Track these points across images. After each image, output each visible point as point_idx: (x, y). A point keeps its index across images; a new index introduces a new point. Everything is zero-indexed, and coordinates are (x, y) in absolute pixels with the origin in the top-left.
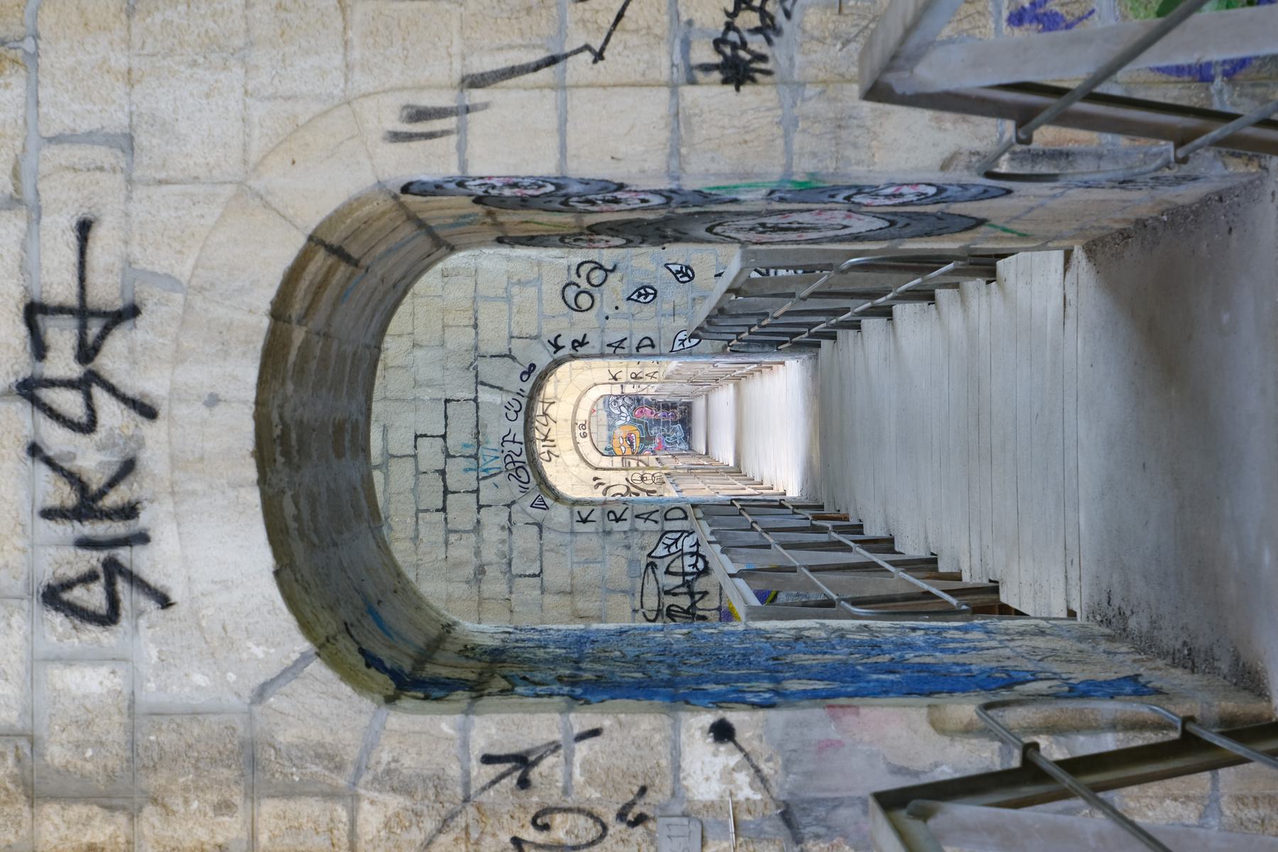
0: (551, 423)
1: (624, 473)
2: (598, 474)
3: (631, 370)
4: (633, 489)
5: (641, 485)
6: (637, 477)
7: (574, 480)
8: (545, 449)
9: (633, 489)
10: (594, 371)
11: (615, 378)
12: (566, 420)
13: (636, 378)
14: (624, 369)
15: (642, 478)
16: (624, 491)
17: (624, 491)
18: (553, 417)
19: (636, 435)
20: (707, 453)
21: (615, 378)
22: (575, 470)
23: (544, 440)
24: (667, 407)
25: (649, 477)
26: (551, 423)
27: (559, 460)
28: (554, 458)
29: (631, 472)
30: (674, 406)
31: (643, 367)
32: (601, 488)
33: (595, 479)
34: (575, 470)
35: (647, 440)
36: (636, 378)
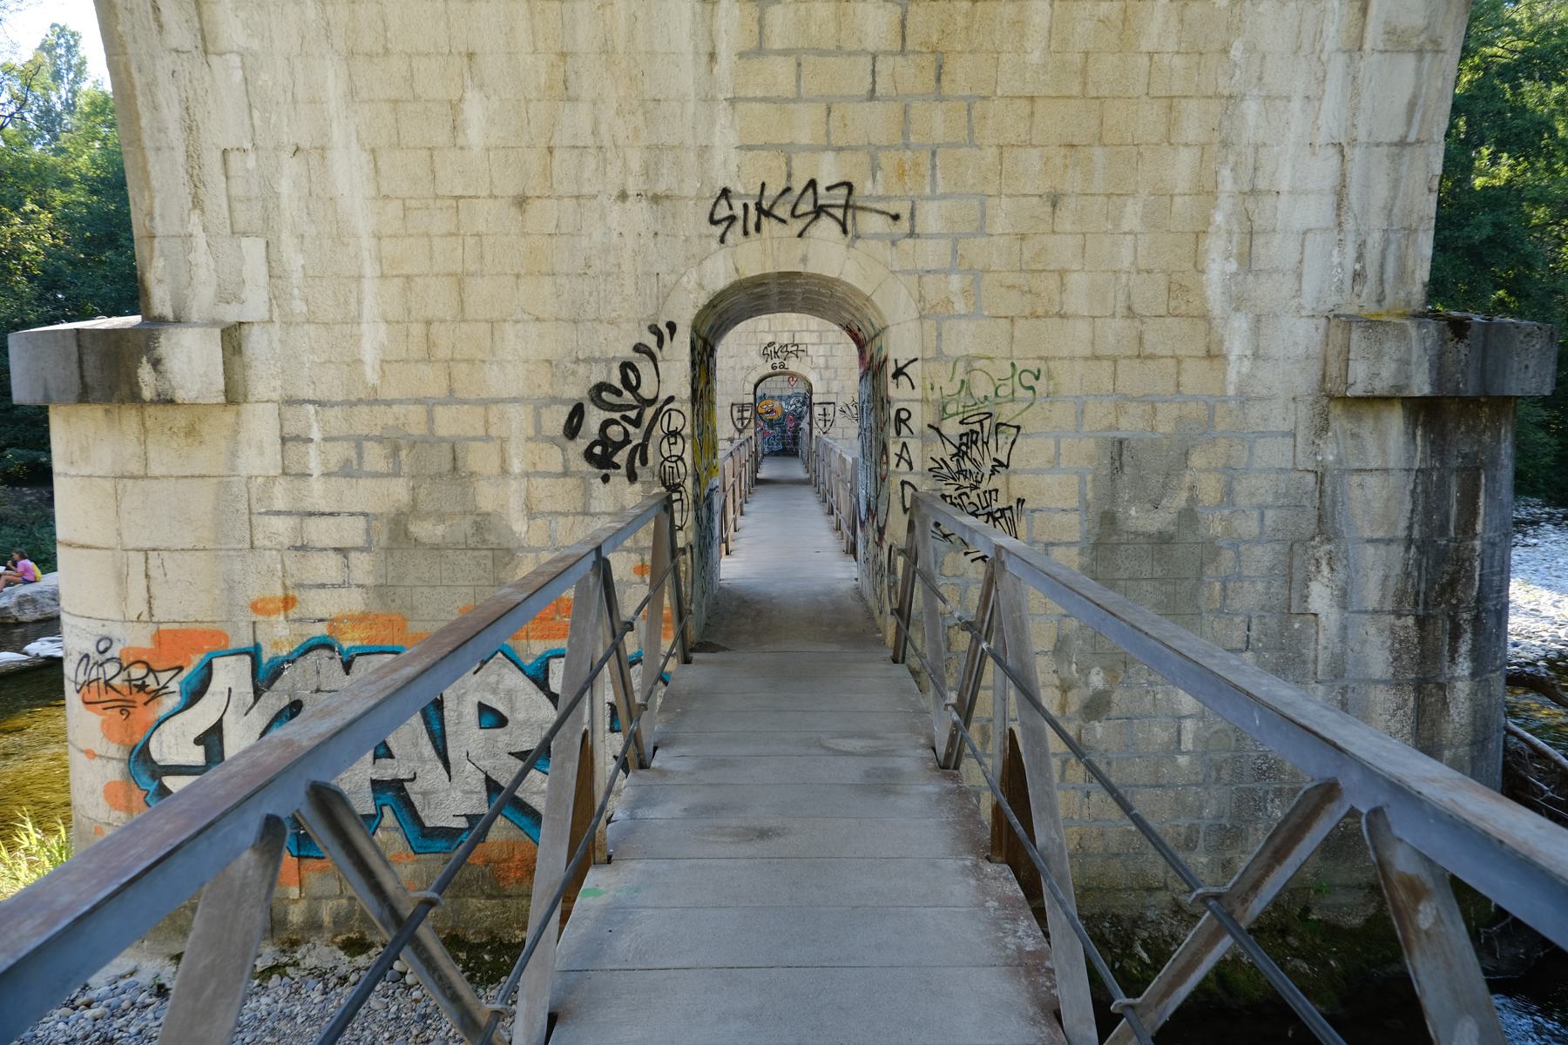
0: (798, 225)
1: (685, 392)
2: (684, 337)
3: (916, 409)
4: (649, 412)
5: (657, 432)
6: (677, 422)
7: (669, 279)
8: (739, 211)
9: (649, 412)
10: (914, 326)
11: (899, 372)
12: (804, 260)
13: (899, 421)
14: (918, 394)
15: (675, 434)
16: (646, 391)
17: (646, 391)
18: (812, 230)
19: (775, 416)
20: (760, 482)
21: (899, 372)
22: (690, 280)
23: (759, 206)
24: (795, 439)
25: (676, 450)
26: (798, 225)
27: (715, 244)
28: (718, 230)
29: (687, 409)
30: (796, 444)
31: (922, 436)
32: (651, 341)
33: (672, 327)
34: (690, 280)
35: (771, 424)
36: (899, 421)
